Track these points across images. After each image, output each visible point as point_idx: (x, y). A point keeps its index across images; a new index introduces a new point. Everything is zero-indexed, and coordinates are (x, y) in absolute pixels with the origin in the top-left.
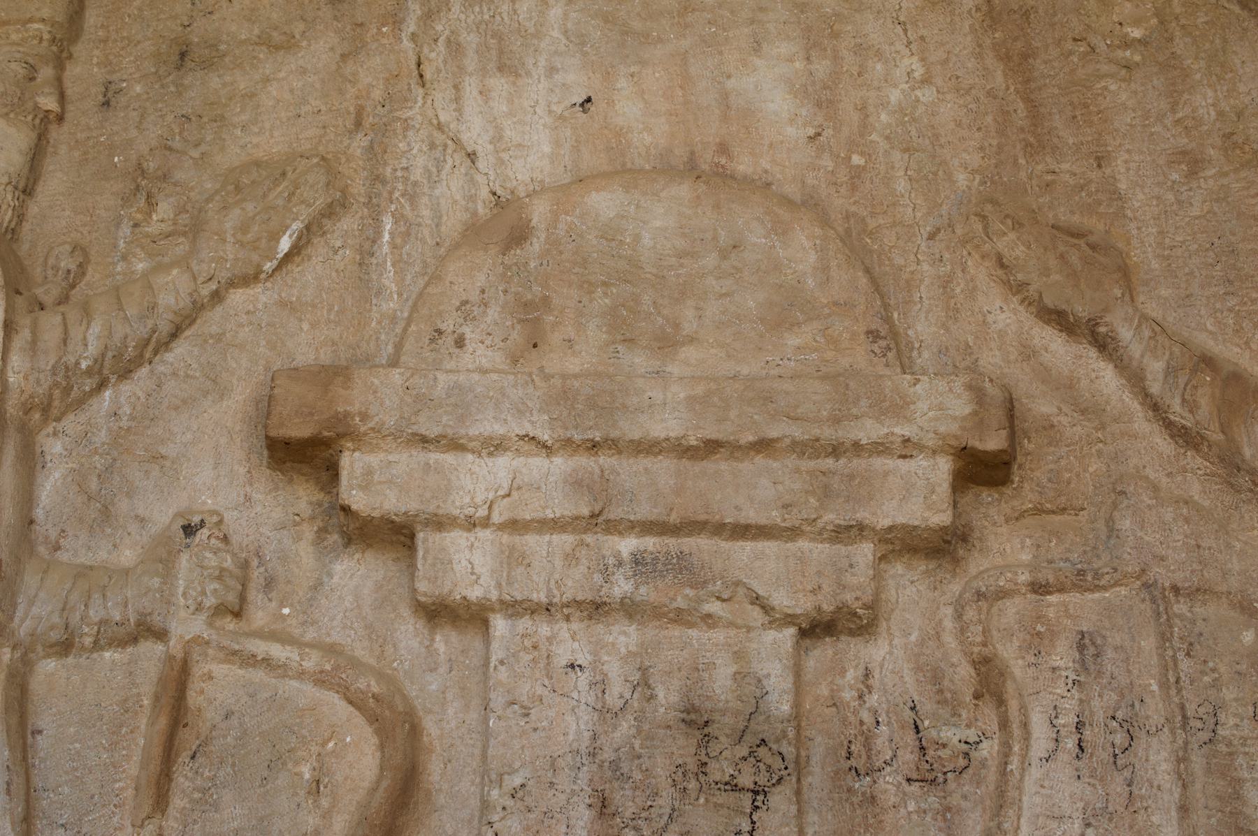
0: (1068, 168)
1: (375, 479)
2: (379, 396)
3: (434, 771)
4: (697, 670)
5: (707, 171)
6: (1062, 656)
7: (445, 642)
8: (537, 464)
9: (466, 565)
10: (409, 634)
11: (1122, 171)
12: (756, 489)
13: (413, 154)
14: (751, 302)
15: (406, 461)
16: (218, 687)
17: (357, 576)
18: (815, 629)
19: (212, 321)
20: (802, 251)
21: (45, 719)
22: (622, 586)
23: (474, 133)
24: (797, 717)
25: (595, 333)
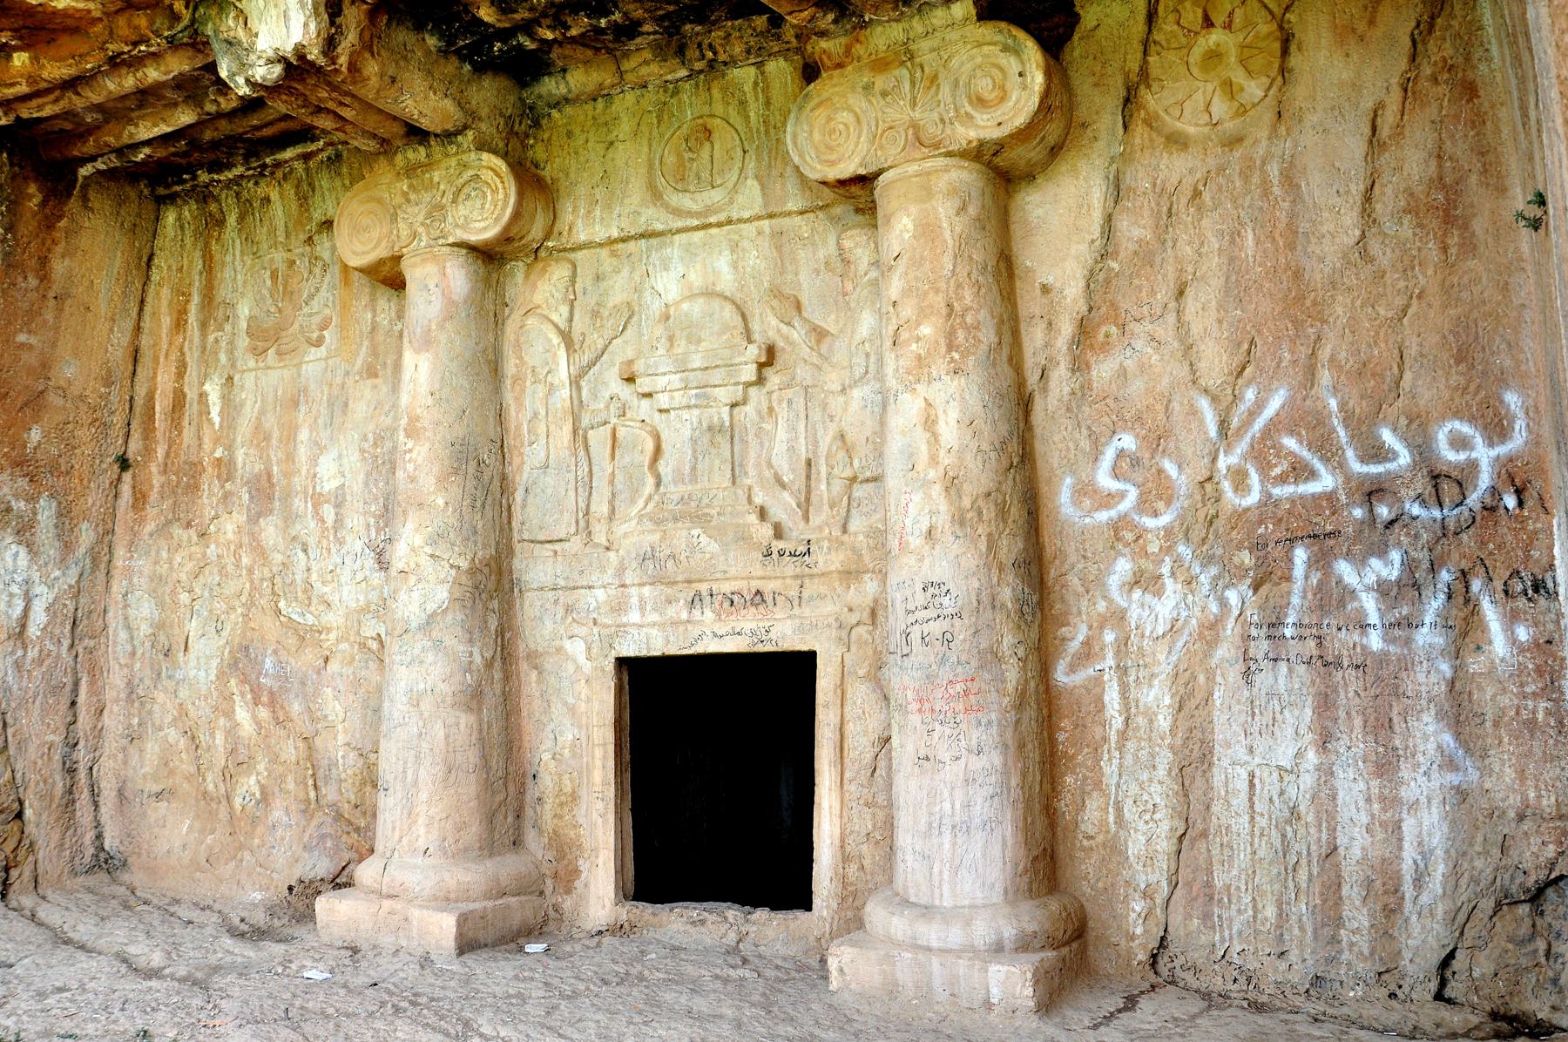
0: (790, 277)
1: (644, 384)
2: (639, 367)
3: (664, 446)
4: (711, 417)
5: (710, 293)
6: (785, 405)
7: (664, 416)
8: (673, 377)
9: (663, 400)
10: (657, 414)
11: (802, 278)
12: (717, 377)
13: (647, 295)
14: (716, 328)
15: (648, 379)
16: (621, 432)
17: (645, 402)
18: (733, 406)
19: (610, 348)
20: (728, 313)
21: (591, 442)
22: (693, 402)
23: (660, 289)
24: (732, 426)
25: (683, 342)
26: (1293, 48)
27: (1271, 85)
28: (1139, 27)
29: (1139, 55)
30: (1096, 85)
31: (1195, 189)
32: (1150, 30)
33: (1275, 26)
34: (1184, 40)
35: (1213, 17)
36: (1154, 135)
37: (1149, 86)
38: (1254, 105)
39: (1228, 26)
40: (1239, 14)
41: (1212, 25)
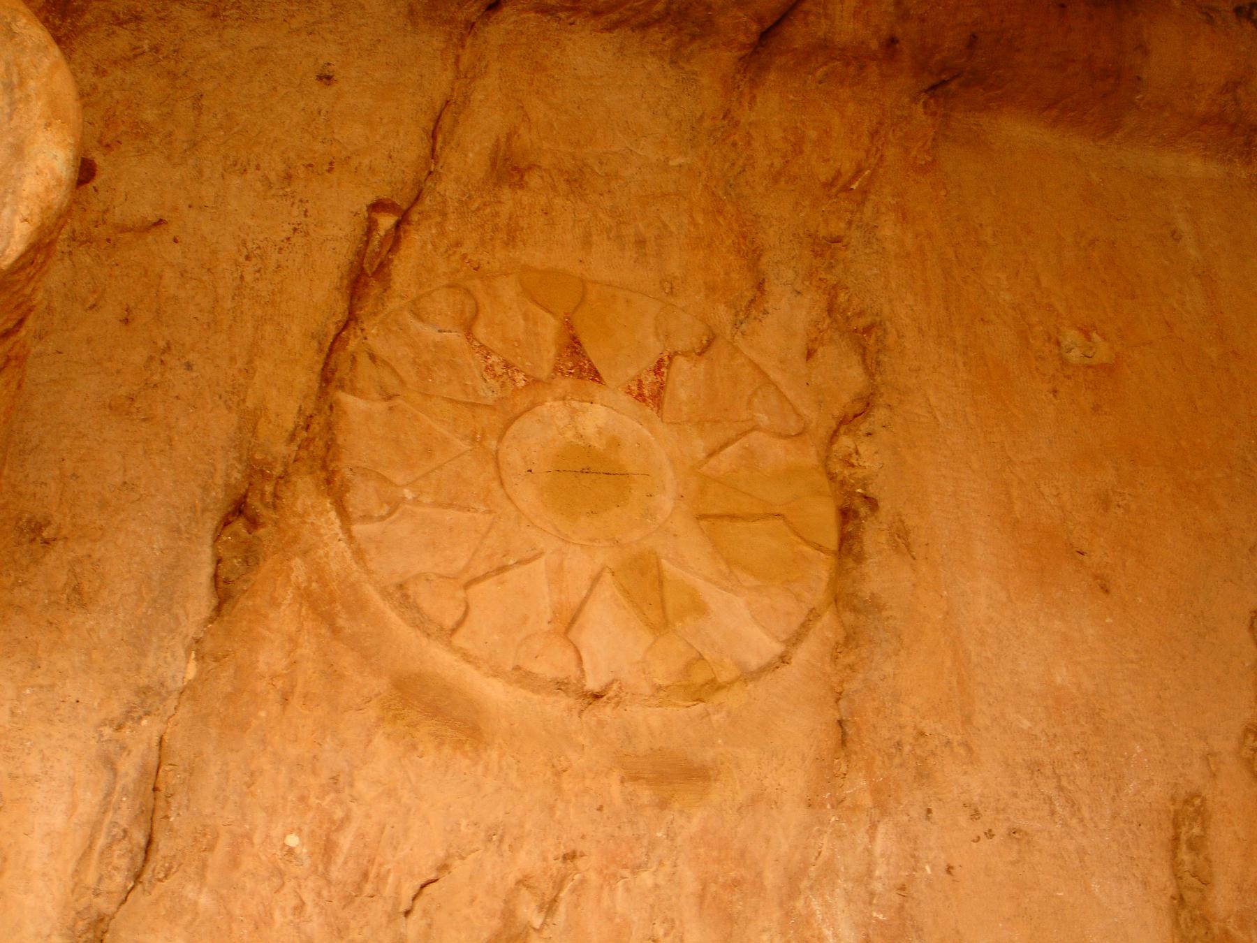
26: (874, 536)
27: (805, 626)
28: (316, 292)
29: (305, 378)
30: (122, 408)
31: (508, 915)
32: (351, 319)
33: (810, 458)
34: (488, 391)
35: (596, 352)
36: (347, 661)
37: (334, 488)
38: (748, 676)
39: (651, 394)
40: (686, 380)
41: (596, 376)
